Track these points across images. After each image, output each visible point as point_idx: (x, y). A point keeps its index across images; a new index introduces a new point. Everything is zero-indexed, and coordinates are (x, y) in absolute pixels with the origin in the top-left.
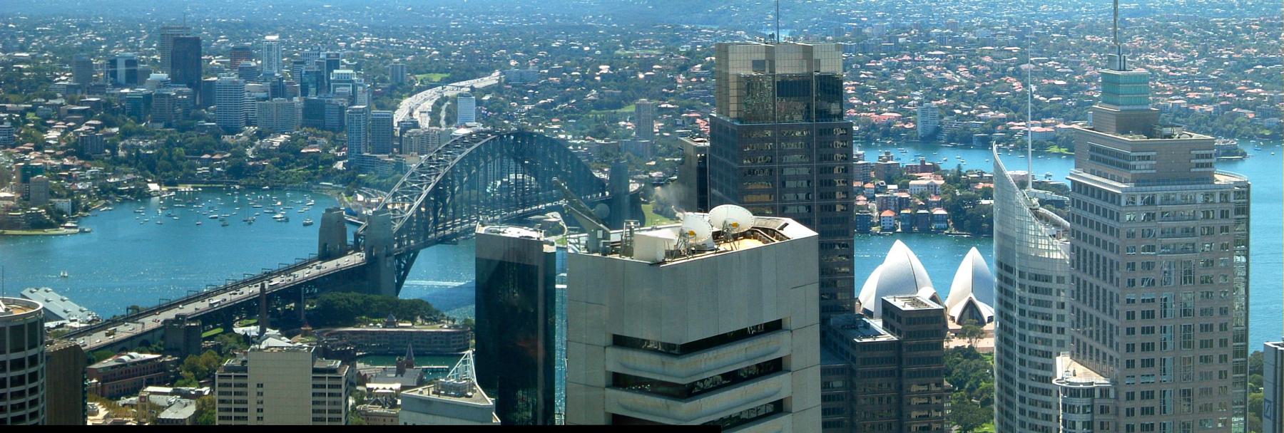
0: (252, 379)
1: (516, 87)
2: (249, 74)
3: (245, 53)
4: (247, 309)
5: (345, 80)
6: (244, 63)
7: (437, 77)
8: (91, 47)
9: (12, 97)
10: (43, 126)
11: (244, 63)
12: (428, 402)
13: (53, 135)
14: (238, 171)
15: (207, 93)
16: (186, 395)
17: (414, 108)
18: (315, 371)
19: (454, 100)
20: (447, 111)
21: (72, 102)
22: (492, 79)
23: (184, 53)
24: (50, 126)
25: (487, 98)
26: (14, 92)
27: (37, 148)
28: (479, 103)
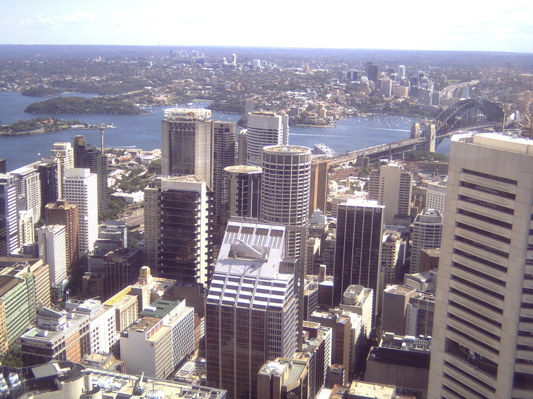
0: (381, 176)
1: (483, 85)
2: (393, 78)
3: (391, 71)
4: (385, 154)
5: (425, 81)
6: (392, 74)
7: (457, 81)
8: (343, 68)
9: (316, 83)
10: (326, 93)
11: (392, 74)
12: (436, 187)
13: (329, 96)
14: (387, 109)
15: (378, 84)
16: (362, 180)
17: (448, 93)
18: (402, 174)
19: (462, 89)
20: (458, 93)
21: (335, 85)
22: (477, 82)
23: (373, 71)
24: (328, 93)
25: (473, 88)
26: (317, 81)
27: (323, 100)
28: (470, 90)
